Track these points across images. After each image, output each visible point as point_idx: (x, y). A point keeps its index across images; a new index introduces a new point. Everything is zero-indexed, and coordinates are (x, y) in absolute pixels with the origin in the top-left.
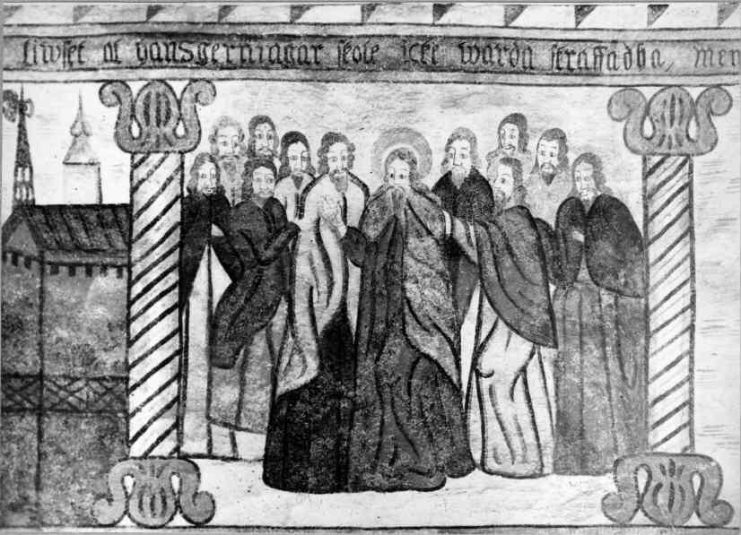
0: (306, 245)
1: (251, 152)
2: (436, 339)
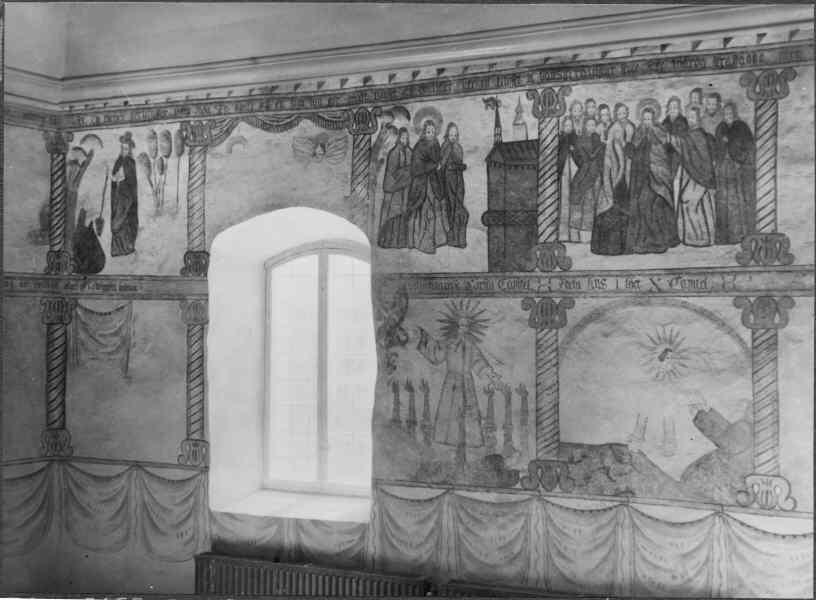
0: (609, 151)
1: (586, 113)
2: (663, 188)
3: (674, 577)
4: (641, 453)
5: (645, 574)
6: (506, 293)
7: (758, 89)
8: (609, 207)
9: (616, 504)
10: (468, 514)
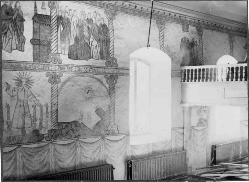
1: (65, 11)
2: (87, 40)
3: (91, 159)
4: (82, 123)
5: (84, 160)
6: (40, 70)
7: (109, 16)
8: (73, 44)
9: (75, 140)
10: (26, 153)
